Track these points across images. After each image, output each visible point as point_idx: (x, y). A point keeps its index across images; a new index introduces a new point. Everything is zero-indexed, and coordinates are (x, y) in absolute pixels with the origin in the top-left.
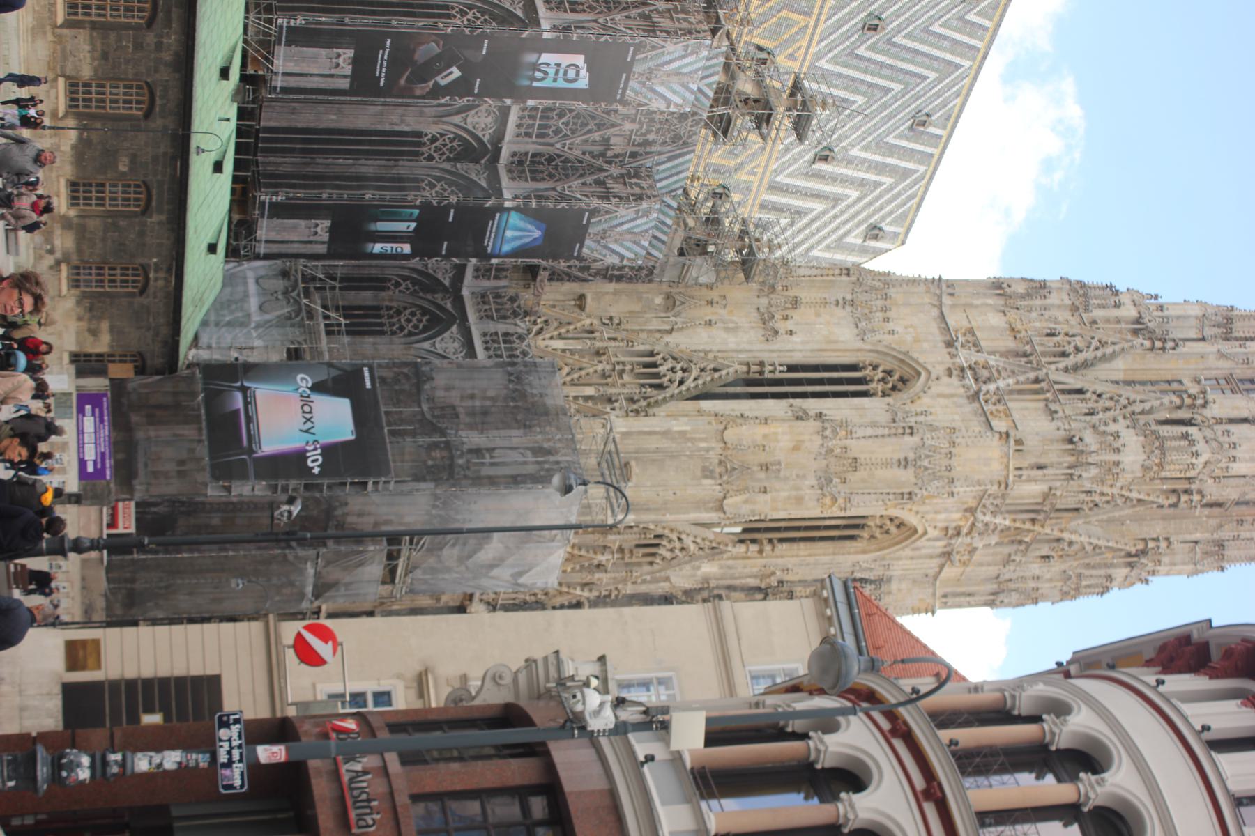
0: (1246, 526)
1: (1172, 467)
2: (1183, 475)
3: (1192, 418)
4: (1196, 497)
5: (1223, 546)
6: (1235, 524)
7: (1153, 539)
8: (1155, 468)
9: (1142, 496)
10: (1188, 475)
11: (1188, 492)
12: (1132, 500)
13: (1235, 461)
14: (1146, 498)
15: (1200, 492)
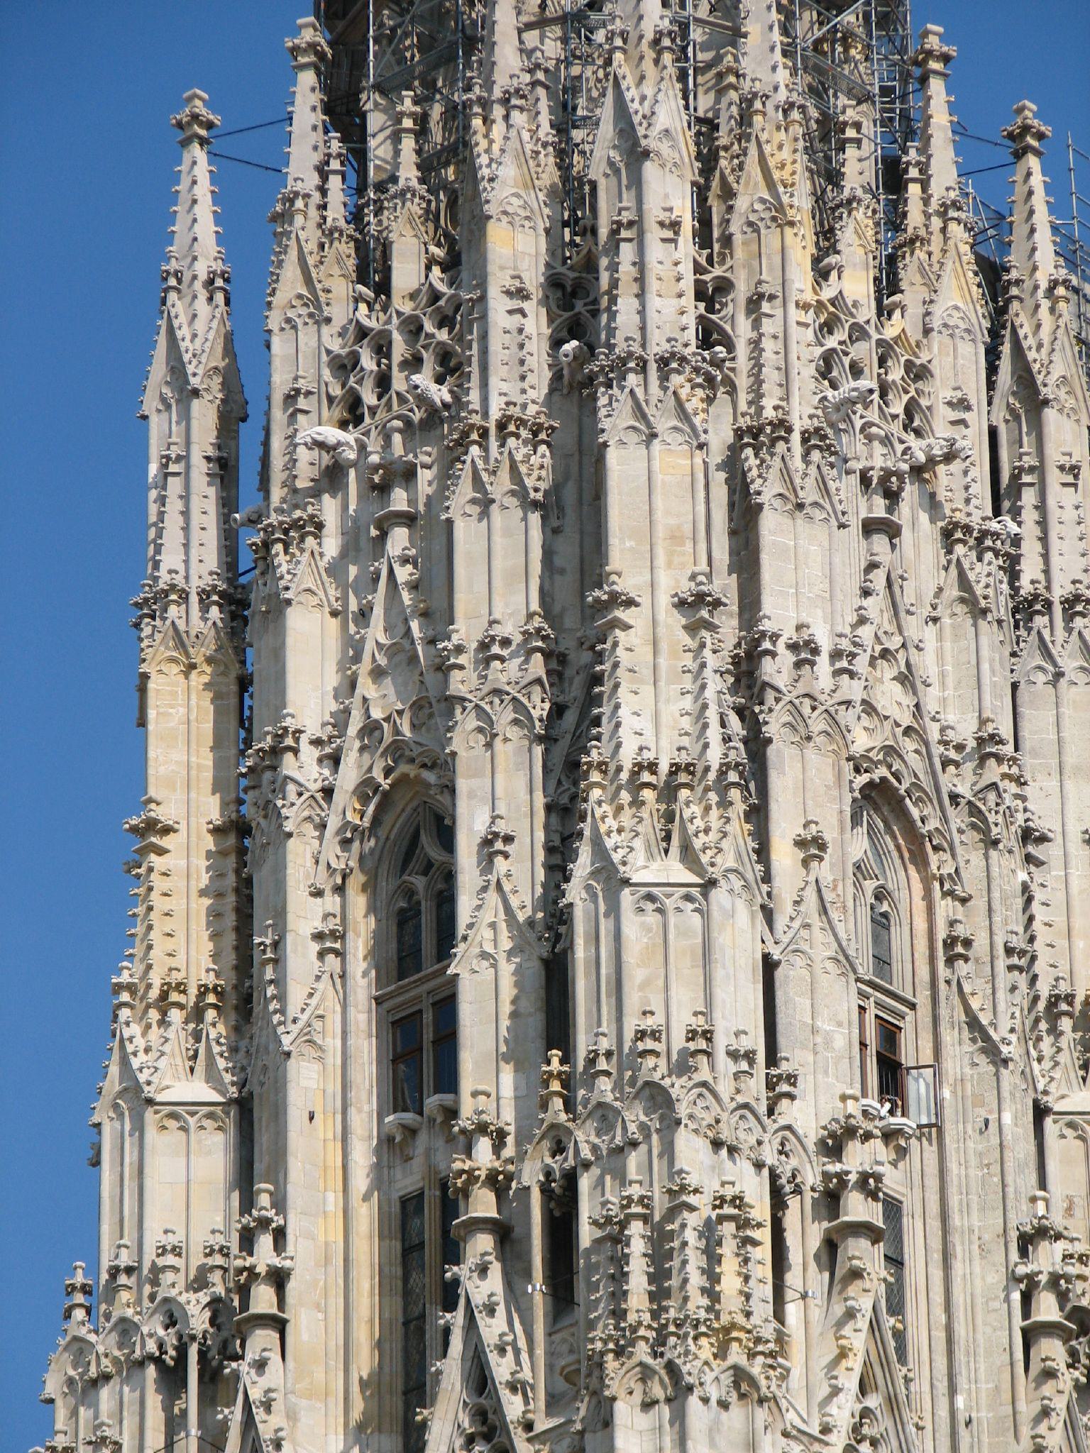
0: (973, 925)
1: (730, 1284)
2: (765, 1235)
3: (545, 1190)
4: (857, 1158)
5: (1054, 1001)
6: (962, 968)
7: (1027, 1299)
8: (736, 1355)
9: (850, 1383)
10: (761, 1210)
11: (831, 1199)
12: (866, 1413)
13: (708, 1035)
14: (855, 1363)
15: (833, 1146)
